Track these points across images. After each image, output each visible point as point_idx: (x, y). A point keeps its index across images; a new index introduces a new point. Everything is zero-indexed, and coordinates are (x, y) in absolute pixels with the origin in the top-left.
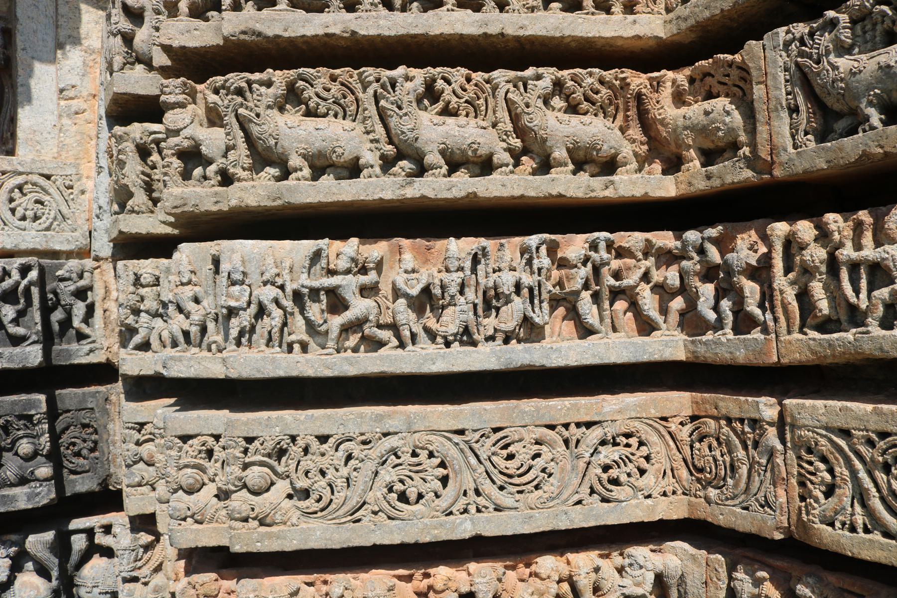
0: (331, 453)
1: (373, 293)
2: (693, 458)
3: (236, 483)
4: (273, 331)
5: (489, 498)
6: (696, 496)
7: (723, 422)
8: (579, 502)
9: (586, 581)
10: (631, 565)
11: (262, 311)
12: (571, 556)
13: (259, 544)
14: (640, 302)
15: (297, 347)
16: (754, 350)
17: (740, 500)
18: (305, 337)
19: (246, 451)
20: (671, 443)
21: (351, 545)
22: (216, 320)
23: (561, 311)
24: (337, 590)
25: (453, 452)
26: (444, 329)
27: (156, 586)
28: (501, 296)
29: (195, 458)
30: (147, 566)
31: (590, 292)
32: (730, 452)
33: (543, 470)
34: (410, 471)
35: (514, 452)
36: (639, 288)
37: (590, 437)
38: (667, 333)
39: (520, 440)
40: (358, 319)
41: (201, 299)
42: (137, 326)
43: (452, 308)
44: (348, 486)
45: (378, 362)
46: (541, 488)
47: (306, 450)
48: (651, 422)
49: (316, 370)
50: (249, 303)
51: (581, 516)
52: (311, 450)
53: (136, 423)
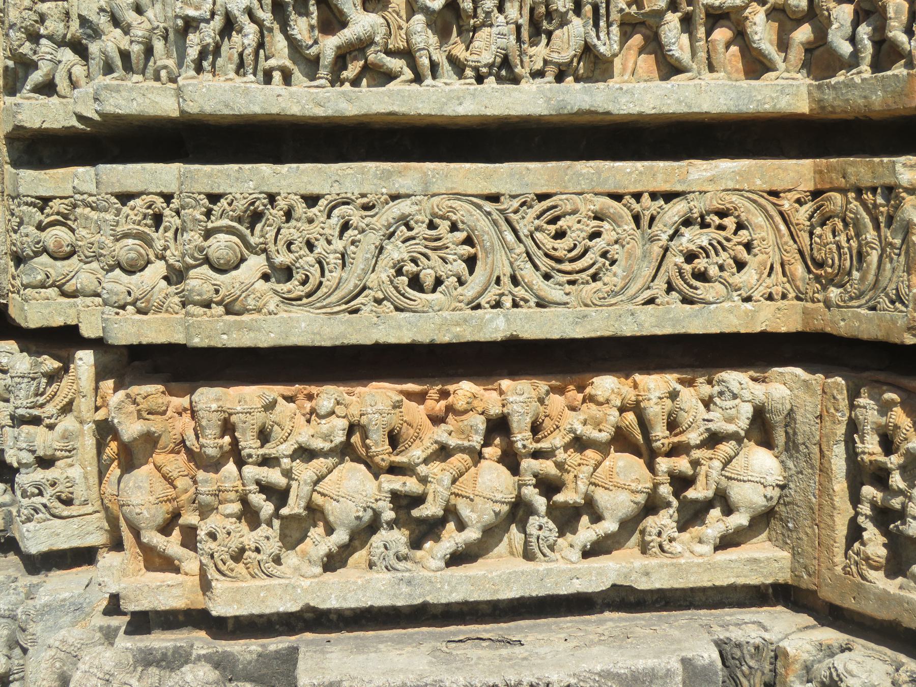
0: (322, 219)
1: (380, 6)
2: (812, 249)
3: (196, 255)
4: (246, 52)
5: (529, 288)
6: (813, 301)
7: (852, 195)
8: (651, 301)
9: (657, 409)
10: (721, 393)
11: (229, 26)
12: (638, 377)
13: (225, 337)
14: (749, 30)
15: (277, 75)
16: (893, 92)
17: (867, 297)
18: (288, 63)
19: (208, 214)
20: (783, 227)
21: (346, 342)
22: (166, 38)
23: (637, 40)
24: (325, 403)
25: (482, 224)
26: (475, 57)
27: (66, 430)
28: (555, 15)
29: (139, 225)
30: (52, 404)
31: (679, 14)
32: (858, 235)
33: (604, 255)
34: (426, 247)
36: (748, 10)
37: (670, 213)
38: (786, 75)
39: (574, 212)
40: (359, 40)
41: (145, 8)
42: (35, 58)
43: (486, 30)
44: (344, 265)
45: (386, 99)
46: (600, 279)
47: (288, 215)
48: (755, 197)
49: (303, 107)
50: (213, 14)
51: (653, 320)
52: (295, 215)
53: (37, 198)
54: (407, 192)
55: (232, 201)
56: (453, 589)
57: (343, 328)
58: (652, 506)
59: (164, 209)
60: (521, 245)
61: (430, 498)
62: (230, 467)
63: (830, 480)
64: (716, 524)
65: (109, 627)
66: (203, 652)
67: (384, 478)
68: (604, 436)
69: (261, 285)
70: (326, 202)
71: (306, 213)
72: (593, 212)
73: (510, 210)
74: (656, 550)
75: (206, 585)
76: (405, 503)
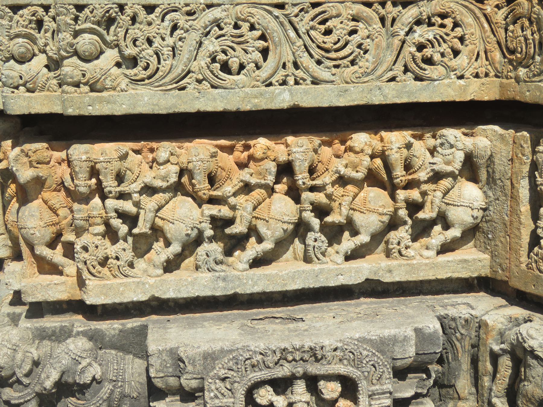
0: (158, 22)
2: (506, 41)
3: (68, 49)
5: (307, 70)
6: (507, 78)
8: (393, 79)
9: (397, 156)
10: (442, 145)
12: (383, 133)
13: (90, 108)
19: (76, 19)
20: (486, 25)
21: (177, 110)
24: (163, 154)
25: (273, 25)
29: (26, 28)
33: (359, 46)
34: (233, 42)
35: (332, 26)
37: (406, 16)
39: (338, 16)
44: (174, 55)
46: (357, 64)
47: (134, 19)
52: (139, 19)
54: (218, 2)
55: (93, 10)
56: (255, 284)
57: (174, 101)
58: (393, 224)
59: (44, 16)
60: (301, 40)
61: (238, 220)
62: (97, 200)
63: (518, 205)
64: (438, 236)
65: (14, 313)
66: (81, 329)
67: (205, 206)
68: (360, 175)
69: (115, 71)
70: (160, 10)
71: (146, 18)
72: (351, 16)
73: (292, 15)
74: (397, 254)
75: (81, 283)
76: (220, 224)
